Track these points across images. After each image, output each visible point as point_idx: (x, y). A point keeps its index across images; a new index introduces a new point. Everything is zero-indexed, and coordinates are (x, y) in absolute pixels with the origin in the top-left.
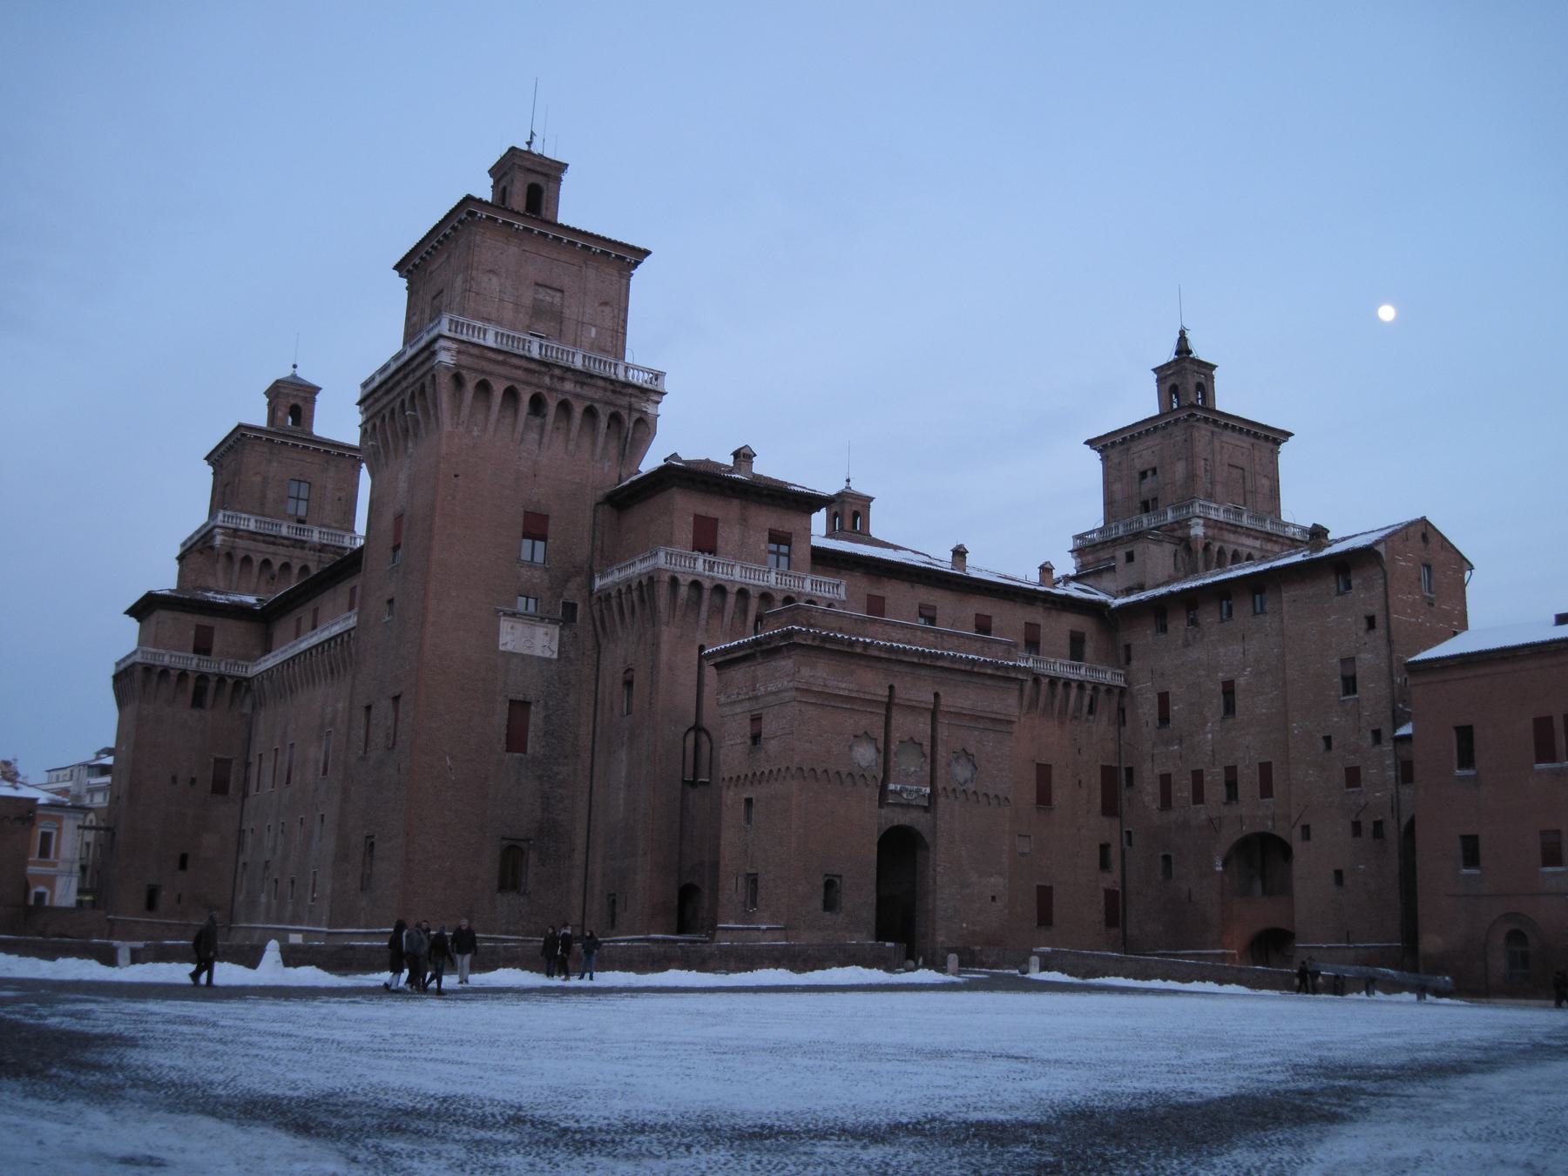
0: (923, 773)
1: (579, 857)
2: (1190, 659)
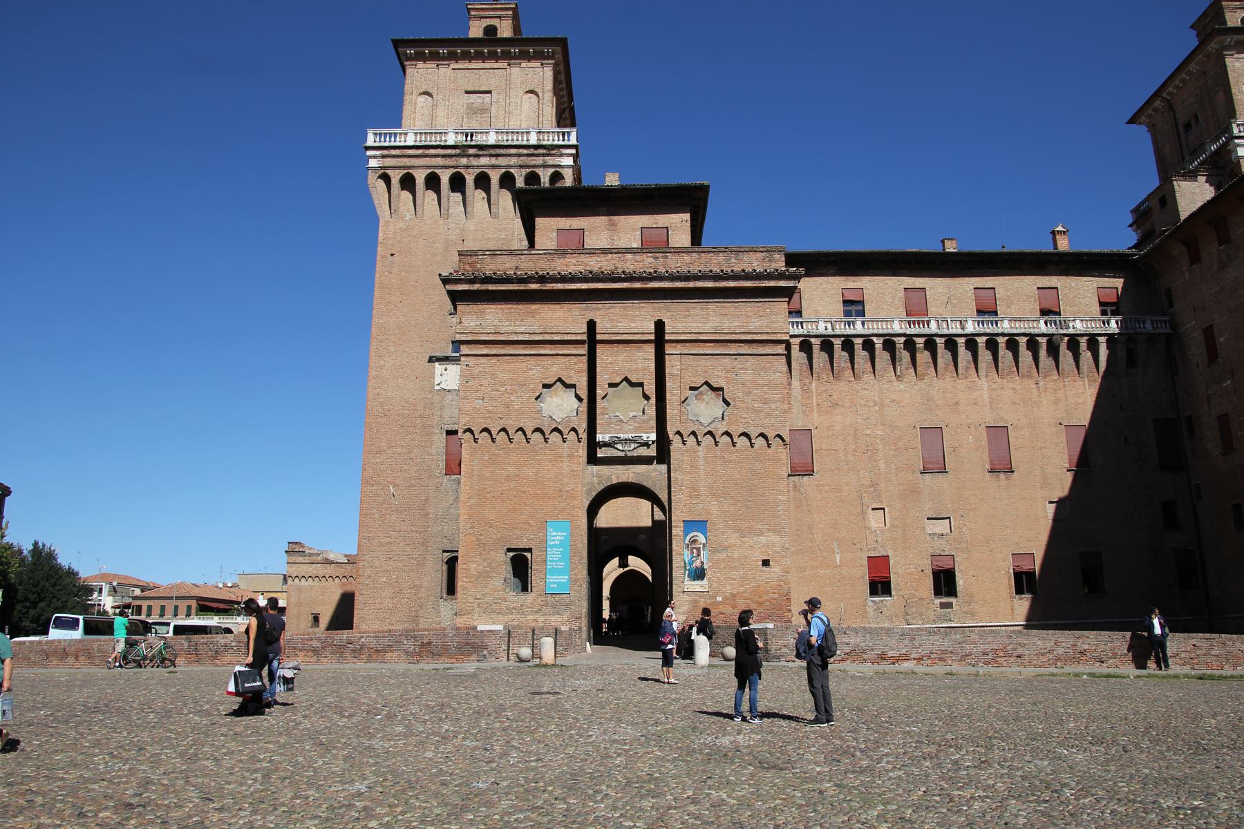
0: (646, 417)
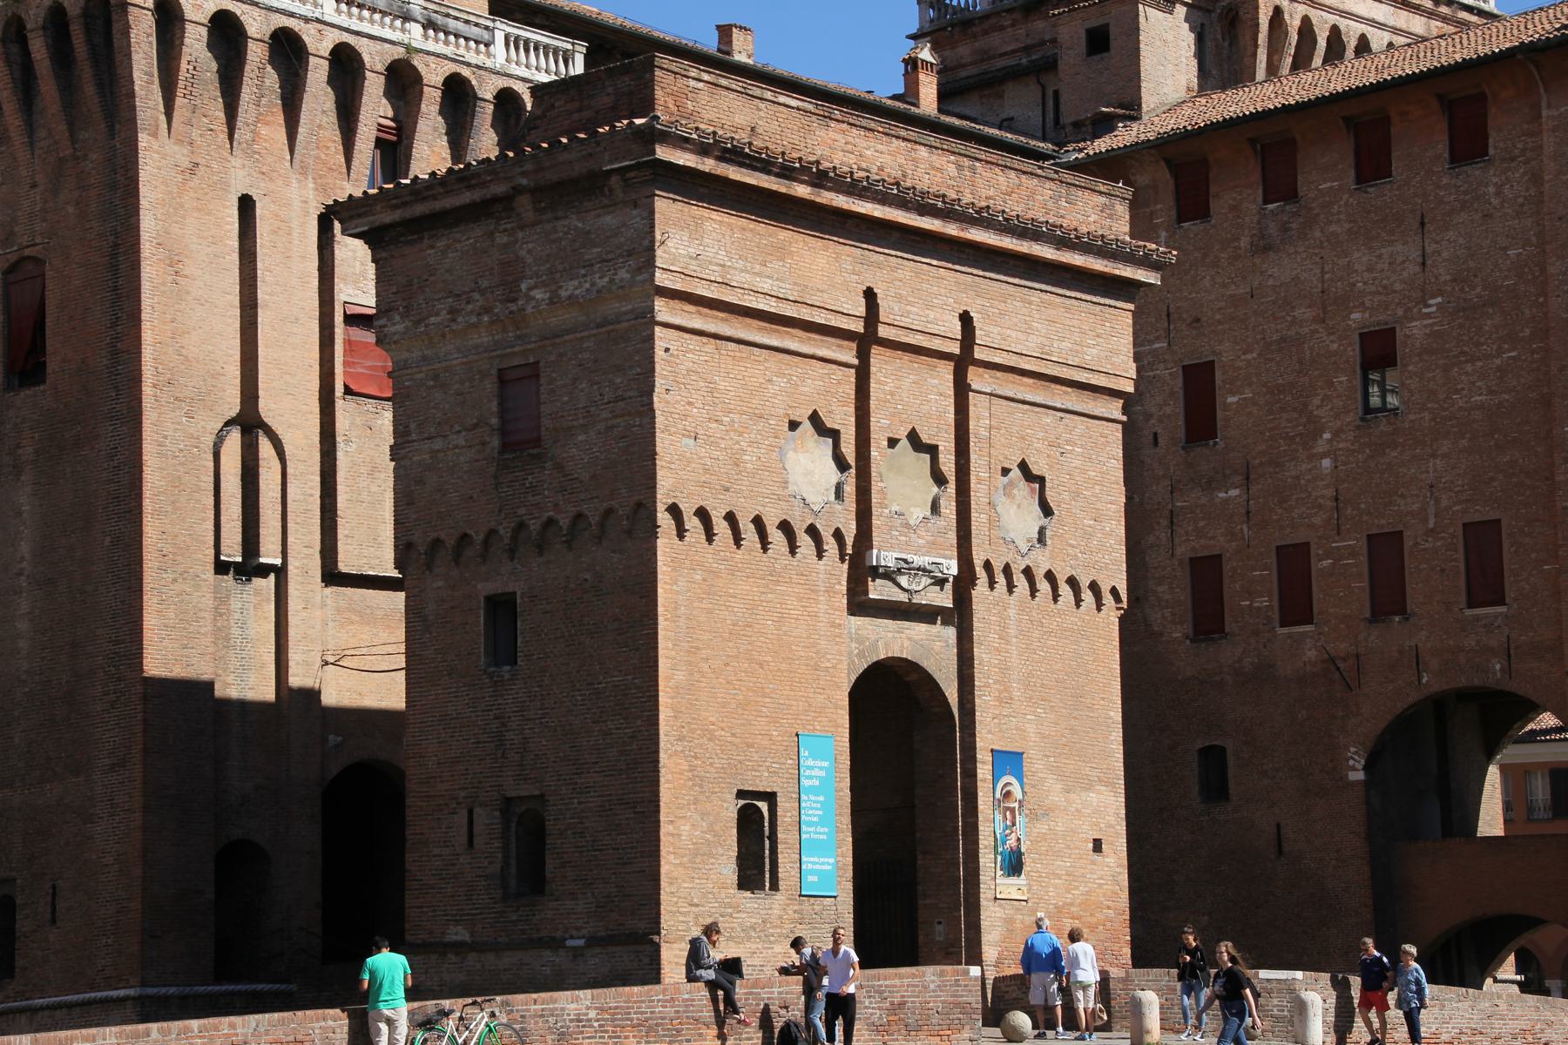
2: (1270, 282)
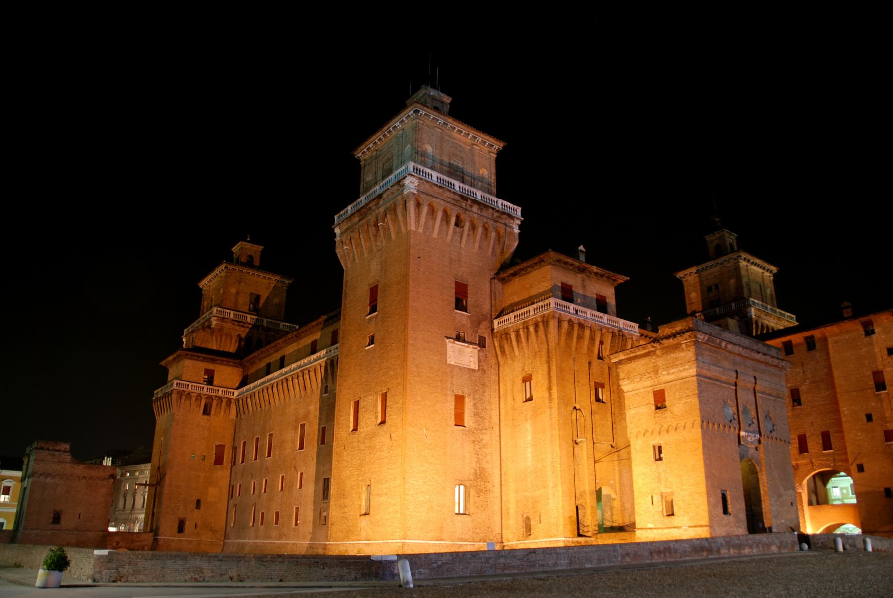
1: (496, 490)
